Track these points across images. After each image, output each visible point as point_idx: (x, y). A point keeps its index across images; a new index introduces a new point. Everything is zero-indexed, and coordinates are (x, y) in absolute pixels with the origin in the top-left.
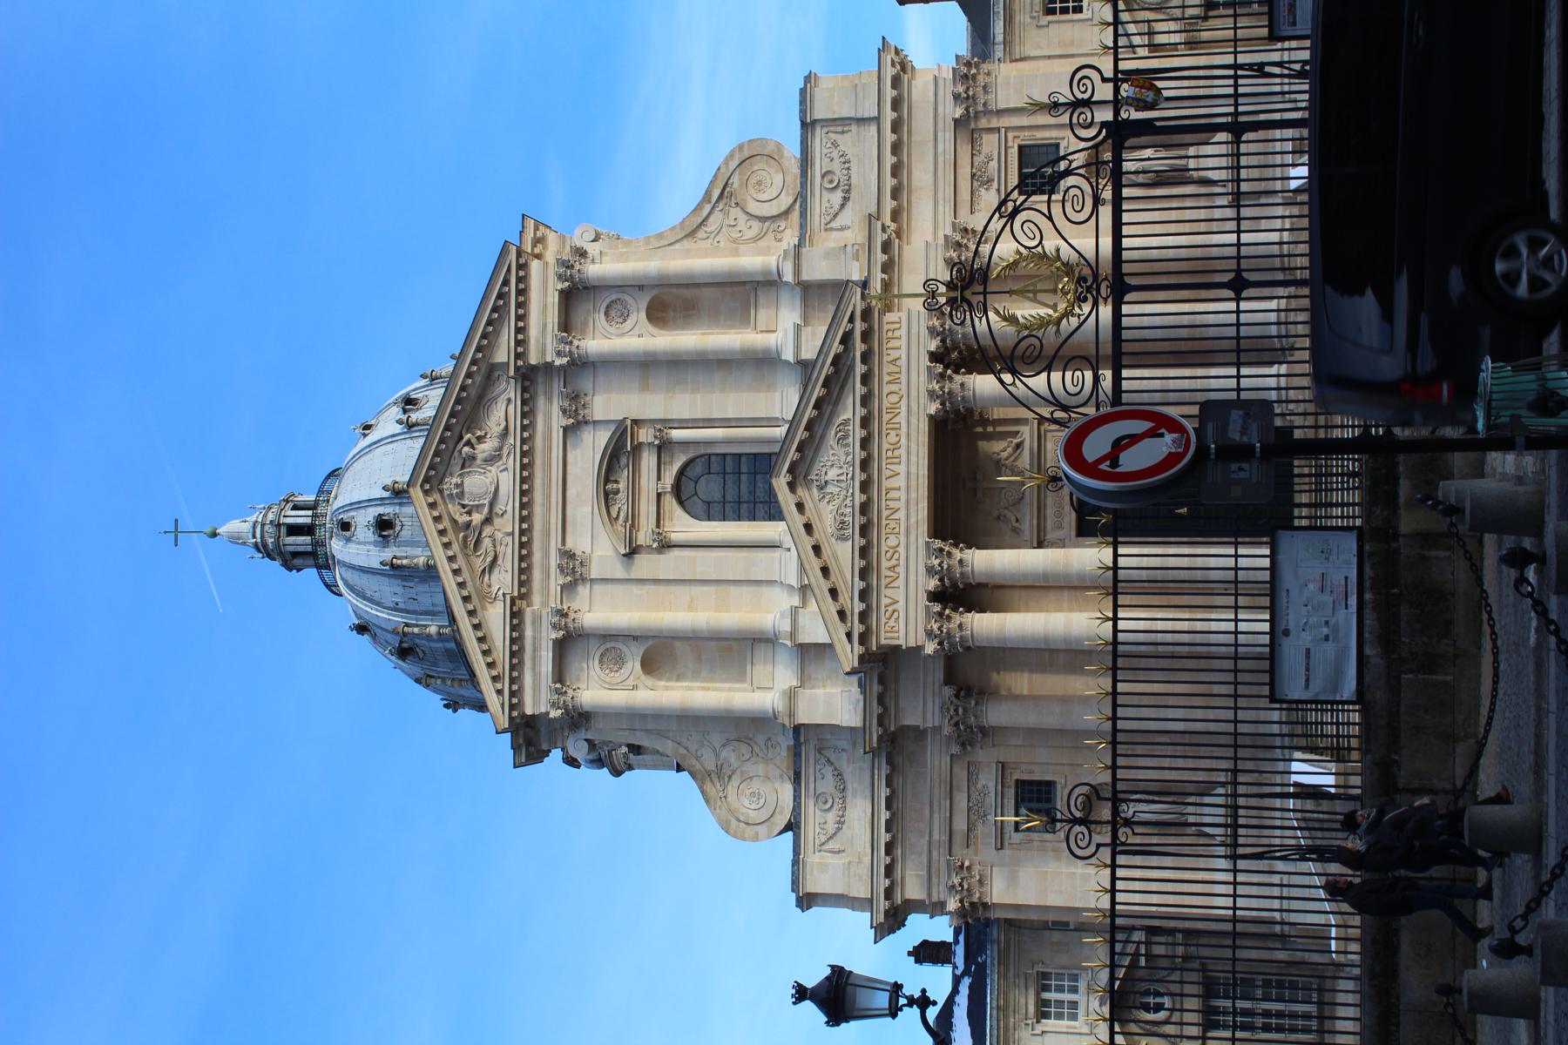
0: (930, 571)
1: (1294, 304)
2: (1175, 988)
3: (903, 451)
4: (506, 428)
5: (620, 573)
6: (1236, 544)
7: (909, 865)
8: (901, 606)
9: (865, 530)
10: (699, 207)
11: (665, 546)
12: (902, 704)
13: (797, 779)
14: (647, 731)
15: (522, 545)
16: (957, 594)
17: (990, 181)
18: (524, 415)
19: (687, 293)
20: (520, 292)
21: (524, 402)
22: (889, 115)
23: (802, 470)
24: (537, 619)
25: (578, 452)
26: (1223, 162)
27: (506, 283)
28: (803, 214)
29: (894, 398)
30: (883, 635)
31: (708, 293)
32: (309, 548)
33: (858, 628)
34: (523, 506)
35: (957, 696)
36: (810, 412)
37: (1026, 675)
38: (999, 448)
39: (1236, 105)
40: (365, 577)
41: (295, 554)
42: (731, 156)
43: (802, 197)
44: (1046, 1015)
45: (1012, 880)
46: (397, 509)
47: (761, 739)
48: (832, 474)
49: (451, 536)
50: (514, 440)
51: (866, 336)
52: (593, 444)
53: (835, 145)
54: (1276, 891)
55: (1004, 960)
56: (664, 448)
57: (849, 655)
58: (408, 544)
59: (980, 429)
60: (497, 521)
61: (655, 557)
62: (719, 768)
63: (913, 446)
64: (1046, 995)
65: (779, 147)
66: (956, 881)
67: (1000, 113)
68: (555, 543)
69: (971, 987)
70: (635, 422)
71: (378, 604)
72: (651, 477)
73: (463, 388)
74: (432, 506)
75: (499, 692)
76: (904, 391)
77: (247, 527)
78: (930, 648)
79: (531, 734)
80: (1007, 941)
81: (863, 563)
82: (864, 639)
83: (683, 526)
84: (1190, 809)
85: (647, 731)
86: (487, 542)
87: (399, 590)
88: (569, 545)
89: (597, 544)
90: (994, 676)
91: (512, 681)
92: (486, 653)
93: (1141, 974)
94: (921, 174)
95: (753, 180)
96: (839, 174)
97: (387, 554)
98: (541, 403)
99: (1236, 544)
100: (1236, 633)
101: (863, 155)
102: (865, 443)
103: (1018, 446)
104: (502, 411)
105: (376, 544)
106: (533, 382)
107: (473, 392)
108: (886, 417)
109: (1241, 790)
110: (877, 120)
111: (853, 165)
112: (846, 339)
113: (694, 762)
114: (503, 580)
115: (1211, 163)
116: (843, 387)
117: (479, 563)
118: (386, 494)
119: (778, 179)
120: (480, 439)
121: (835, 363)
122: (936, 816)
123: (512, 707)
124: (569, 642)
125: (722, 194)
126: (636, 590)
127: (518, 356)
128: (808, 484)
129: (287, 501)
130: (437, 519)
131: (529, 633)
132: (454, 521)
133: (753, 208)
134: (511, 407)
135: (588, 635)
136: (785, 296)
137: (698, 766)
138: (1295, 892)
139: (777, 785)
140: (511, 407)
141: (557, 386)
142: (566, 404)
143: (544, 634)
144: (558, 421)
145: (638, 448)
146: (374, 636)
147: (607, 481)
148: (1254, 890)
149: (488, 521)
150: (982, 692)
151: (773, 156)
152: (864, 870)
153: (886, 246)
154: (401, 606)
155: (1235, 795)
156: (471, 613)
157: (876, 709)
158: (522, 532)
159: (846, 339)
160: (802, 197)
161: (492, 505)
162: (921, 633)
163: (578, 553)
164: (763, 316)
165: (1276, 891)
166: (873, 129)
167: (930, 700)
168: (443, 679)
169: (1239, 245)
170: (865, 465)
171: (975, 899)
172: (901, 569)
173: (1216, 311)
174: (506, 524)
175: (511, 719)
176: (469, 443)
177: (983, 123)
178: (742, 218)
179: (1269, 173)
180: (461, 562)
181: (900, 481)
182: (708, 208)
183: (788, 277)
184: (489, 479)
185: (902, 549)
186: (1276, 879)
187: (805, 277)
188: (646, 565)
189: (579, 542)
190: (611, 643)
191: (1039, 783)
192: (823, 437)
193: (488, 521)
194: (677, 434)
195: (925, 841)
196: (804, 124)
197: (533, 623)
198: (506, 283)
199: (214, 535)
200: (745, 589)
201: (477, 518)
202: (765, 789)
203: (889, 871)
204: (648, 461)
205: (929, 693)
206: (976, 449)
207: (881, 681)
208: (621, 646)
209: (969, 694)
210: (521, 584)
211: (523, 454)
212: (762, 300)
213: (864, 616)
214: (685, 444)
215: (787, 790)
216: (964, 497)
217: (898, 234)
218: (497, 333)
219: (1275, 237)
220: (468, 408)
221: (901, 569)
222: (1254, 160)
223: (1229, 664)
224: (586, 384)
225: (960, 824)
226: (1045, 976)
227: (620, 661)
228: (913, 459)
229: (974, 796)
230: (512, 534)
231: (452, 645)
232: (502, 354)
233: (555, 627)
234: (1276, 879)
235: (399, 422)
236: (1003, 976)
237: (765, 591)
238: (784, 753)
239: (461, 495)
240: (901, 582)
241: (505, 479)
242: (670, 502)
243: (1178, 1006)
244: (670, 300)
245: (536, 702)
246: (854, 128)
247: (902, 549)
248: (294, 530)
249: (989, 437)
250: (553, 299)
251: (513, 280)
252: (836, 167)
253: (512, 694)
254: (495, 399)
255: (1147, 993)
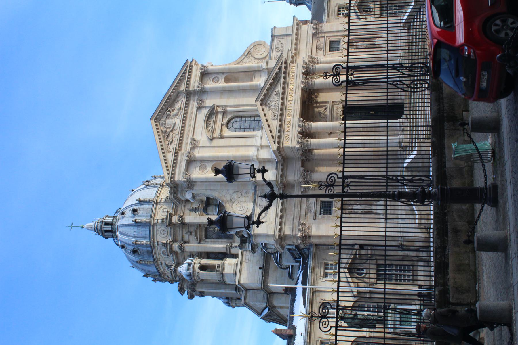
0: (299, 126)
1: (404, 58)
2: (367, 266)
3: (293, 98)
4: (181, 107)
5: (208, 145)
6: (387, 103)
7: (287, 224)
8: (290, 137)
9: (281, 115)
10: (241, 57)
11: (222, 137)
12: (288, 174)
13: (255, 201)
14: (211, 190)
15: (181, 137)
16: (306, 134)
17: (321, 49)
18: (186, 104)
19: (236, 75)
20: (189, 72)
21: (186, 101)
22: (295, 31)
23: (264, 102)
24: (182, 155)
25: (200, 115)
26: (385, 42)
27: (186, 70)
28: (270, 57)
29: (292, 85)
30: (284, 144)
31: (241, 75)
32: (110, 229)
33: (277, 140)
34: (182, 127)
35: (305, 171)
36: (268, 86)
37: (325, 168)
38: (321, 110)
39: (388, 75)
40: (126, 228)
41: (106, 231)
42: (251, 45)
43: (270, 54)
44: (326, 277)
45: (318, 228)
46: (139, 206)
47: (244, 191)
48: (273, 103)
49: (160, 133)
50: (182, 110)
51: (286, 68)
52: (204, 112)
53: (280, 41)
54: (399, 230)
55: (314, 258)
56: (225, 113)
57: (274, 147)
58: (141, 216)
59: (315, 105)
60: (174, 132)
61: (219, 140)
62: (231, 200)
63: (297, 96)
64: (326, 271)
65: (265, 42)
66: (301, 228)
67: (325, 33)
68: (190, 136)
69: (303, 274)
70: (218, 106)
71: (129, 236)
72: (220, 120)
73: (170, 96)
74: (156, 125)
75: (168, 174)
76: (295, 83)
77: (93, 224)
78: (298, 146)
79: (175, 189)
80: (316, 252)
81: (280, 123)
82: (279, 143)
83: (227, 133)
84: (376, 43)
85: (211, 190)
86: (170, 136)
87: (136, 230)
88: (194, 137)
89: (202, 136)
90: (316, 169)
91: (173, 170)
92: (166, 163)
93: (357, 261)
94: (303, 46)
95: (257, 50)
96: (280, 48)
97: (134, 219)
98: (191, 102)
99: (387, 103)
100: (387, 151)
101: (287, 44)
102: (283, 93)
103: (326, 108)
104: (180, 103)
105: (131, 217)
106: (190, 97)
107: (173, 98)
108: (289, 90)
109: (390, 42)
110: (291, 35)
111: (284, 46)
112: (280, 69)
113: (224, 198)
114: (175, 145)
115: (378, 207)
116: (278, 82)
117: (167, 142)
118: (137, 202)
119: (264, 50)
120: (173, 110)
121: (276, 74)
122: (296, 210)
123: (171, 178)
124: (190, 162)
125: (248, 54)
126: (212, 149)
127: (187, 87)
128: (266, 105)
129: (106, 216)
130: (157, 129)
131: (179, 158)
132: (162, 131)
133: (256, 56)
134: (183, 103)
135: (197, 160)
136: (263, 74)
137: (225, 199)
138: (405, 230)
139: (248, 203)
140: (183, 103)
141: (196, 97)
142: (198, 102)
143: (184, 158)
144: (195, 105)
145: (217, 113)
146: (125, 250)
147: (207, 121)
148: (392, 230)
149: (171, 131)
150: (312, 172)
151: (263, 44)
152: (273, 226)
153: (292, 57)
154: (136, 235)
155: (386, 210)
156: (163, 153)
157: (280, 173)
158: (181, 133)
159: (280, 69)
160: (270, 54)
161: (173, 127)
162: (296, 142)
163: (197, 139)
164: (256, 79)
165: (399, 230)
166: (290, 37)
167: (296, 172)
168: (145, 261)
169: (385, 289)
170: (283, 99)
171: (306, 234)
172: (291, 127)
173: (382, 74)
174: (177, 132)
175: (171, 181)
176: (169, 111)
177: (320, 35)
178: (253, 59)
179: (397, 45)
180: (162, 140)
181: (292, 105)
182: (244, 57)
183: (265, 67)
184: (174, 121)
185: (291, 122)
186: (399, 225)
187: (269, 67)
188: (215, 142)
189: (197, 137)
190: (203, 161)
191: (327, 214)
192: (271, 94)
193: (171, 131)
194: (229, 109)
195: (292, 217)
196: (272, 36)
197: (181, 155)
198: (186, 70)
199: (83, 227)
200: (244, 148)
201: (168, 130)
202: (245, 205)
203: (281, 224)
204: (220, 116)
205: (296, 170)
206: (314, 110)
207: (282, 165)
208: (206, 164)
209: (308, 171)
210: (179, 147)
211: (185, 114)
212: (256, 75)
213: (279, 137)
214: (231, 112)
215: (251, 205)
216: (309, 107)
217: (295, 55)
218: (182, 83)
219: (399, 55)
220: (171, 102)
221: (291, 127)
222: (393, 38)
223: (385, 157)
224: (204, 97)
225: (303, 213)
226: (327, 265)
227: (205, 168)
228: (296, 99)
229: (308, 204)
230: (178, 135)
231: (149, 249)
232: (182, 88)
233: (187, 156)
234: (399, 225)
235: (144, 185)
236: (314, 262)
237: (250, 148)
238: (251, 195)
239: (165, 124)
240: (290, 130)
241: (178, 121)
242: (225, 127)
243: (368, 272)
244: (230, 75)
245: (179, 177)
246: (285, 37)
247: (291, 122)
248: (107, 224)
249: (318, 107)
250: (199, 74)
251: (188, 69)
252: (280, 46)
253: (172, 174)
254: (178, 101)
255: (358, 269)
